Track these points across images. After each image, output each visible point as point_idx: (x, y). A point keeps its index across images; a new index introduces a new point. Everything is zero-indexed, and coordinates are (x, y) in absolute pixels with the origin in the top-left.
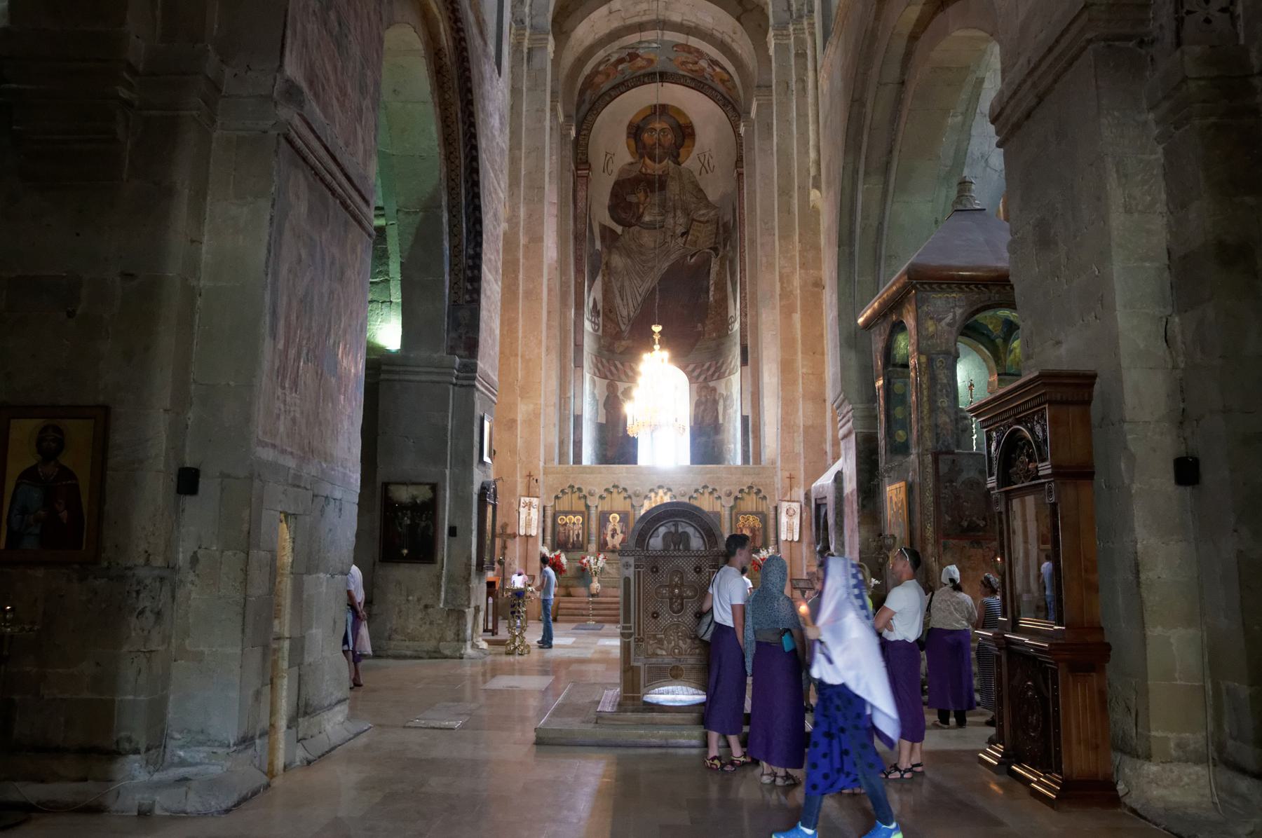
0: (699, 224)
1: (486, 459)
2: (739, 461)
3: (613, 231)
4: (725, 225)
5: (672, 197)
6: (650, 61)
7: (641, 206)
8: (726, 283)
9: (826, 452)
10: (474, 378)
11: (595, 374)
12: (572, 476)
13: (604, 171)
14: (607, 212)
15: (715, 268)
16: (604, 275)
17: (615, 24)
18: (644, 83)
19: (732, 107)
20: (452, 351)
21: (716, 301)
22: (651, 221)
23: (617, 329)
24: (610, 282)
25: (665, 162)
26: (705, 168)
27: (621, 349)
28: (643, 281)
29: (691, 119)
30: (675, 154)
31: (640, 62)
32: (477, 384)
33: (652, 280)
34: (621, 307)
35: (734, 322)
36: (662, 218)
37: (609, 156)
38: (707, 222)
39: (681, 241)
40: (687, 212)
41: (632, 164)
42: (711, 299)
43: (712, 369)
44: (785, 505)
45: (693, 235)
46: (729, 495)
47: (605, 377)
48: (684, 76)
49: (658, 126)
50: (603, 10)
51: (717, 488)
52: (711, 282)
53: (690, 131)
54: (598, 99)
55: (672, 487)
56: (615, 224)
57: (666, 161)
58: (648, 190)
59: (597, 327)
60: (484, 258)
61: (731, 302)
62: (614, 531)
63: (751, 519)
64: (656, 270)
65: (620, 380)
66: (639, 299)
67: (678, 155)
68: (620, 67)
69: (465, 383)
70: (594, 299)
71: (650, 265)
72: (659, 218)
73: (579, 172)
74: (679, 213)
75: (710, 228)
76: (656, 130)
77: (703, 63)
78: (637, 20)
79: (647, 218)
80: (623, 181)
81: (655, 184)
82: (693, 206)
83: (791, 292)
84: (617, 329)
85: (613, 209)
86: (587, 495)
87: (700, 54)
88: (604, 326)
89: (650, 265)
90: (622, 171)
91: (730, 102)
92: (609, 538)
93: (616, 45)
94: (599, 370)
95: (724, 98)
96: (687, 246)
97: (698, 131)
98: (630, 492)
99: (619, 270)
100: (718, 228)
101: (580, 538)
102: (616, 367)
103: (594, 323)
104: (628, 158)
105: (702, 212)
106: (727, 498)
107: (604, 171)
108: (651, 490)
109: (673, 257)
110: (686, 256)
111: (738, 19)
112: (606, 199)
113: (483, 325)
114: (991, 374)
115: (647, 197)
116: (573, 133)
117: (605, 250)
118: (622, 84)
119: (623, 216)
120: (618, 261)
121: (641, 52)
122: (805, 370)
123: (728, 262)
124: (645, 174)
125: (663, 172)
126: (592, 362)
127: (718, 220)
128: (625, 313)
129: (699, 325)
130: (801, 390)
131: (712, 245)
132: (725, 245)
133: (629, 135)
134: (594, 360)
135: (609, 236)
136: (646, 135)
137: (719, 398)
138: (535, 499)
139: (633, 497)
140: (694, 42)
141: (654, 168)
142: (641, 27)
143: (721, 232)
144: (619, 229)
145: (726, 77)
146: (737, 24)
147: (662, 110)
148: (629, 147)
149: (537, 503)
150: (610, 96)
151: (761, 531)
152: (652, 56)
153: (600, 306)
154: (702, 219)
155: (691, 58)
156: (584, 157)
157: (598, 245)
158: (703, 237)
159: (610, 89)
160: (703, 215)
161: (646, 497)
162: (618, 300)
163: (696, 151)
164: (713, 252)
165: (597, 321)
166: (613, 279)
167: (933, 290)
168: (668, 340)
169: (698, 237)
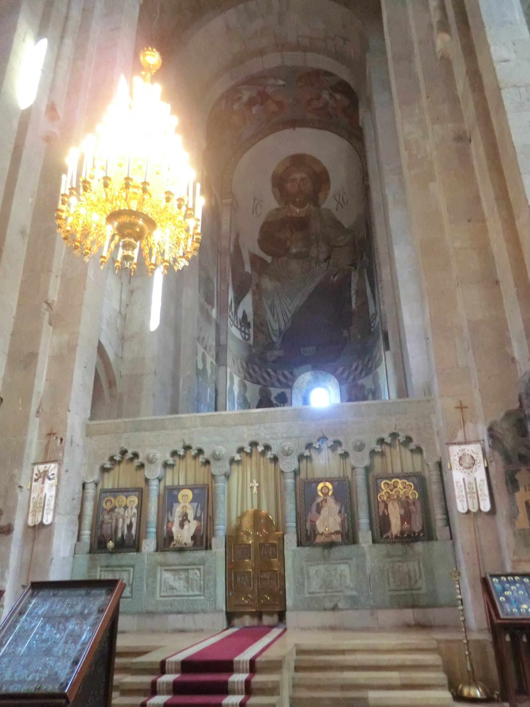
8: (365, 288)
9: (513, 359)
11: (245, 378)
12: (125, 436)
15: (355, 279)
16: (254, 294)
23: (269, 340)
24: (260, 299)
27: (273, 358)
34: (273, 323)
35: (375, 319)
39: (324, 266)
41: (277, 209)
42: (354, 306)
44: (455, 451)
46: (360, 448)
47: (258, 383)
51: (341, 439)
52: (353, 292)
55: (271, 443)
59: (247, 337)
62: (184, 518)
63: (400, 486)
65: (273, 385)
66: (290, 316)
70: (244, 312)
72: (303, 250)
79: (294, 250)
84: (269, 340)
86: (146, 463)
88: (255, 336)
92: (175, 529)
94: (251, 376)
101: (133, 531)
103: (245, 333)
106: (359, 454)
109: (318, 280)
120: (268, 284)
126: (243, 367)
128: (276, 327)
129: (345, 331)
134: (244, 365)
137: (369, 393)
138: (53, 465)
139: (212, 462)
144: (269, 259)
149: (55, 472)
151: (418, 504)
153: (250, 319)
157: (248, 268)
162: (269, 316)
165: (247, 331)
166: (264, 299)
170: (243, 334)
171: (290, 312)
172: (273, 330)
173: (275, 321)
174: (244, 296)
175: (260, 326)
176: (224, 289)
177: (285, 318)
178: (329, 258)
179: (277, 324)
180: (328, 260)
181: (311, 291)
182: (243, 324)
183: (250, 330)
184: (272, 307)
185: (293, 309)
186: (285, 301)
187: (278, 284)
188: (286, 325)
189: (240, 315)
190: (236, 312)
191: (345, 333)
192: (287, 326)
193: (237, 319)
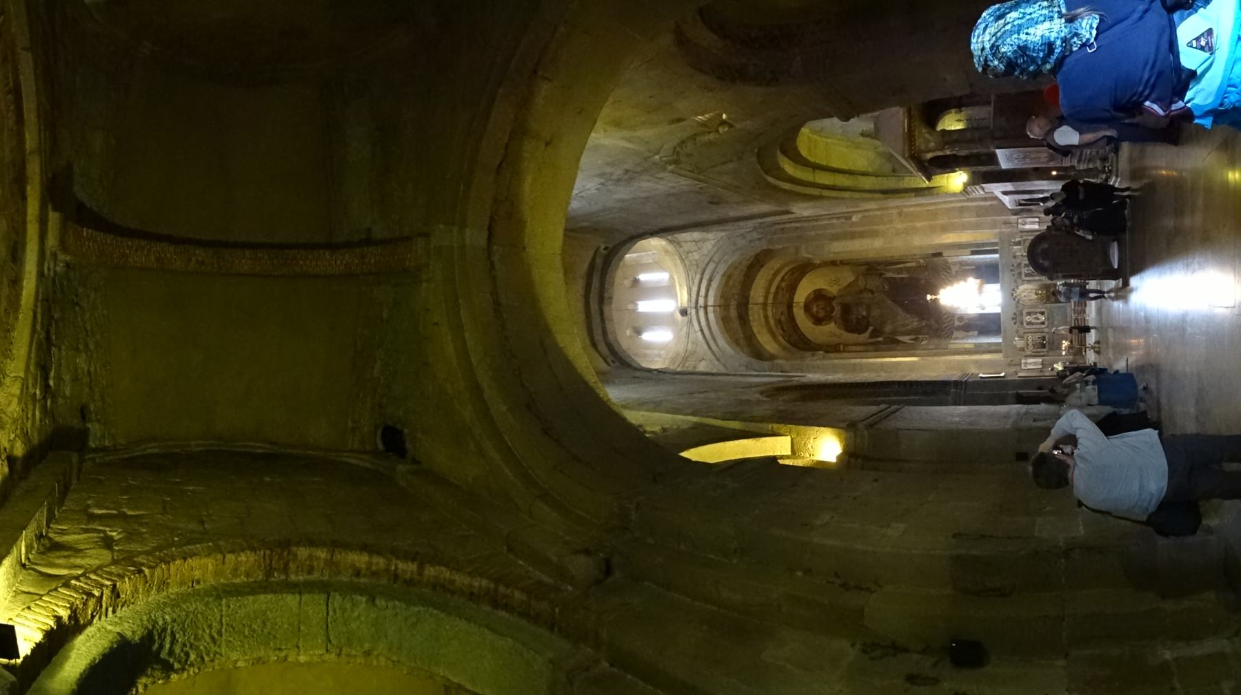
1: (1002, 375)
2: (997, 256)
3: (873, 331)
4: (869, 270)
6: (782, 313)
10: (961, 382)
11: (951, 338)
15: (889, 275)
16: (897, 336)
17: (765, 330)
19: (804, 268)
20: (948, 394)
25: (835, 305)
26: (837, 281)
31: (783, 319)
32: (965, 379)
39: (876, 295)
40: (861, 292)
41: (835, 323)
42: (907, 276)
43: (946, 274)
47: (952, 332)
48: (790, 296)
50: (758, 336)
51: (1011, 264)
52: (897, 276)
60: (899, 380)
61: (909, 265)
65: (954, 324)
66: (908, 316)
68: (785, 328)
69: (964, 386)
72: (864, 306)
74: (862, 296)
77: (783, 284)
78: (763, 320)
81: (846, 309)
83: (904, 228)
85: (860, 332)
87: (778, 287)
88: (923, 334)
90: (840, 329)
93: (774, 328)
98: (1015, 311)
102: (946, 327)
104: (833, 324)
108: (1014, 299)
111: (762, 266)
112: (856, 335)
113: (934, 379)
114: (951, 113)
116: (821, 352)
120: (888, 328)
121: (777, 318)
122: (946, 218)
130: (956, 220)
135: (875, 333)
140: (773, 290)
141: (837, 311)
142: (766, 317)
144: (871, 328)
145: (790, 273)
146: (765, 266)
147: (807, 308)
148: (826, 324)
152: (780, 313)
153: (913, 337)
154: (864, 283)
155: (780, 292)
157: (880, 339)
158: (874, 283)
161: (1018, 302)
162: (909, 327)
167: (914, 145)
168: (934, 293)
184: (904, 325)
189: (913, 342)
191: (923, 282)
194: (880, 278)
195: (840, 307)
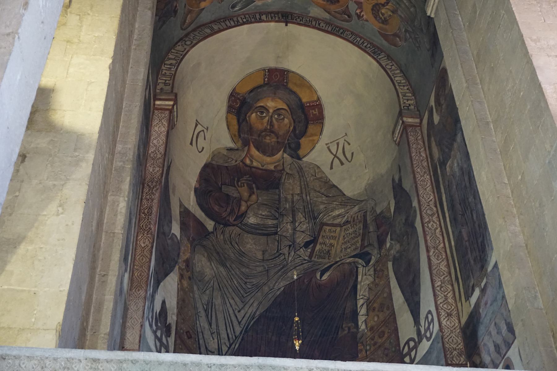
0: (334, 229)
5: (289, 197)
7: (243, 203)
13: (191, 144)
14: (193, 193)
16: (181, 277)
18: (261, 21)
21: (372, 329)
22: (258, 224)
28: (245, 304)
29: (320, 93)
30: (293, 146)
33: (260, 303)
34: (207, 334)
35: (416, 347)
36: (275, 222)
37: (199, 128)
38: (347, 222)
39: (304, 253)
40: (312, 215)
41: (230, 149)
42: (363, 327)
45: (324, 243)
48: (316, 19)
49: (271, 104)
52: (360, 302)
53: (316, 112)
54: (194, 30)
56: (203, 214)
57: (281, 152)
58: (254, 186)
64: (266, 289)
66: (238, 330)
67: (298, 146)
70: (164, 302)
71: (254, 281)
72: (270, 222)
73: (158, 103)
74: (300, 216)
75: (351, 231)
76: (268, 111)
79: (252, 220)
80: (219, 167)
82: (322, 207)
89: (254, 281)
90: (214, 155)
91: (382, 51)
95: (374, 46)
96: (313, 259)
97: (327, 113)
99: (207, 279)
100: (365, 226)
103: (160, 340)
105: (337, 212)
107: (191, 144)
110: (314, 272)
112: (193, 180)
115: (251, 193)
117: (185, 241)
118: (230, 18)
119: (216, 208)
123: (390, 264)
124: (251, 167)
125: (275, 167)
127: (365, 216)
131: (358, 251)
132: (381, 243)
133: (230, 109)
136: (254, 115)
143: (371, 229)
144: (210, 225)
150: (212, 29)
153: (172, 319)
154: (337, 221)
156: (168, 88)
157: (176, 229)
159: (211, 22)
160: (339, 215)
162: (203, 322)
163: (325, 138)
164: (360, 261)
166: (195, 288)
169: (332, 245)
170: (158, 344)
171: (239, 323)
172: (206, 348)
173: (212, 334)
174: (166, 275)
175: (186, 337)
176: (143, 245)
177: (229, 331)
178: (313, 242)
179: (216, 340)
180: (312, 245)
181: (278, 293)
182: (159, 324)
183: (169, 339)
184: (209, 308)
185: (246, 319)
186: (232, 301)
187: (222, 269)
188: (231, 345)
190: (153, 297)
192: (233, 346)
193: (153, 309)
194: (354, 256)
195: (272, 167)
